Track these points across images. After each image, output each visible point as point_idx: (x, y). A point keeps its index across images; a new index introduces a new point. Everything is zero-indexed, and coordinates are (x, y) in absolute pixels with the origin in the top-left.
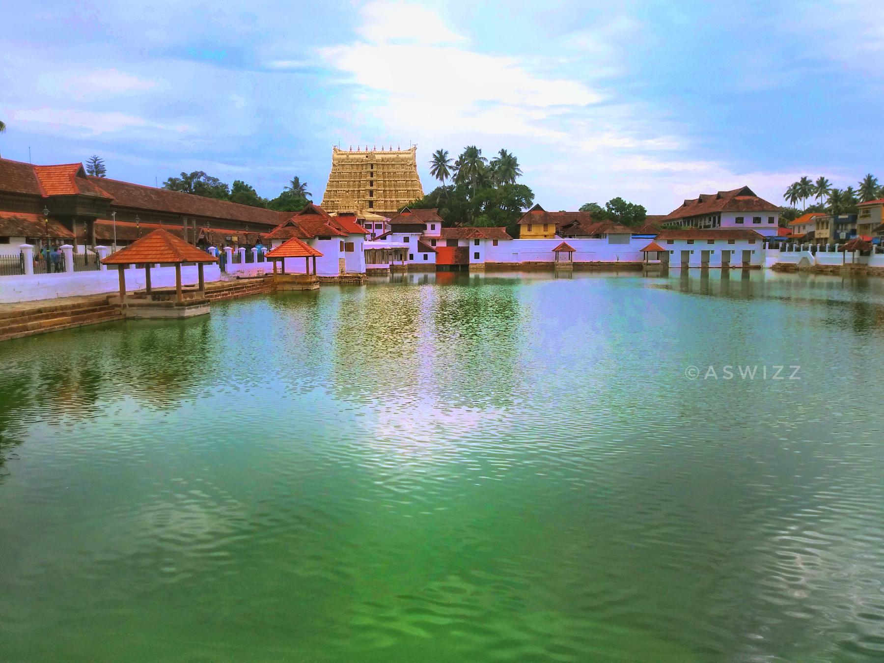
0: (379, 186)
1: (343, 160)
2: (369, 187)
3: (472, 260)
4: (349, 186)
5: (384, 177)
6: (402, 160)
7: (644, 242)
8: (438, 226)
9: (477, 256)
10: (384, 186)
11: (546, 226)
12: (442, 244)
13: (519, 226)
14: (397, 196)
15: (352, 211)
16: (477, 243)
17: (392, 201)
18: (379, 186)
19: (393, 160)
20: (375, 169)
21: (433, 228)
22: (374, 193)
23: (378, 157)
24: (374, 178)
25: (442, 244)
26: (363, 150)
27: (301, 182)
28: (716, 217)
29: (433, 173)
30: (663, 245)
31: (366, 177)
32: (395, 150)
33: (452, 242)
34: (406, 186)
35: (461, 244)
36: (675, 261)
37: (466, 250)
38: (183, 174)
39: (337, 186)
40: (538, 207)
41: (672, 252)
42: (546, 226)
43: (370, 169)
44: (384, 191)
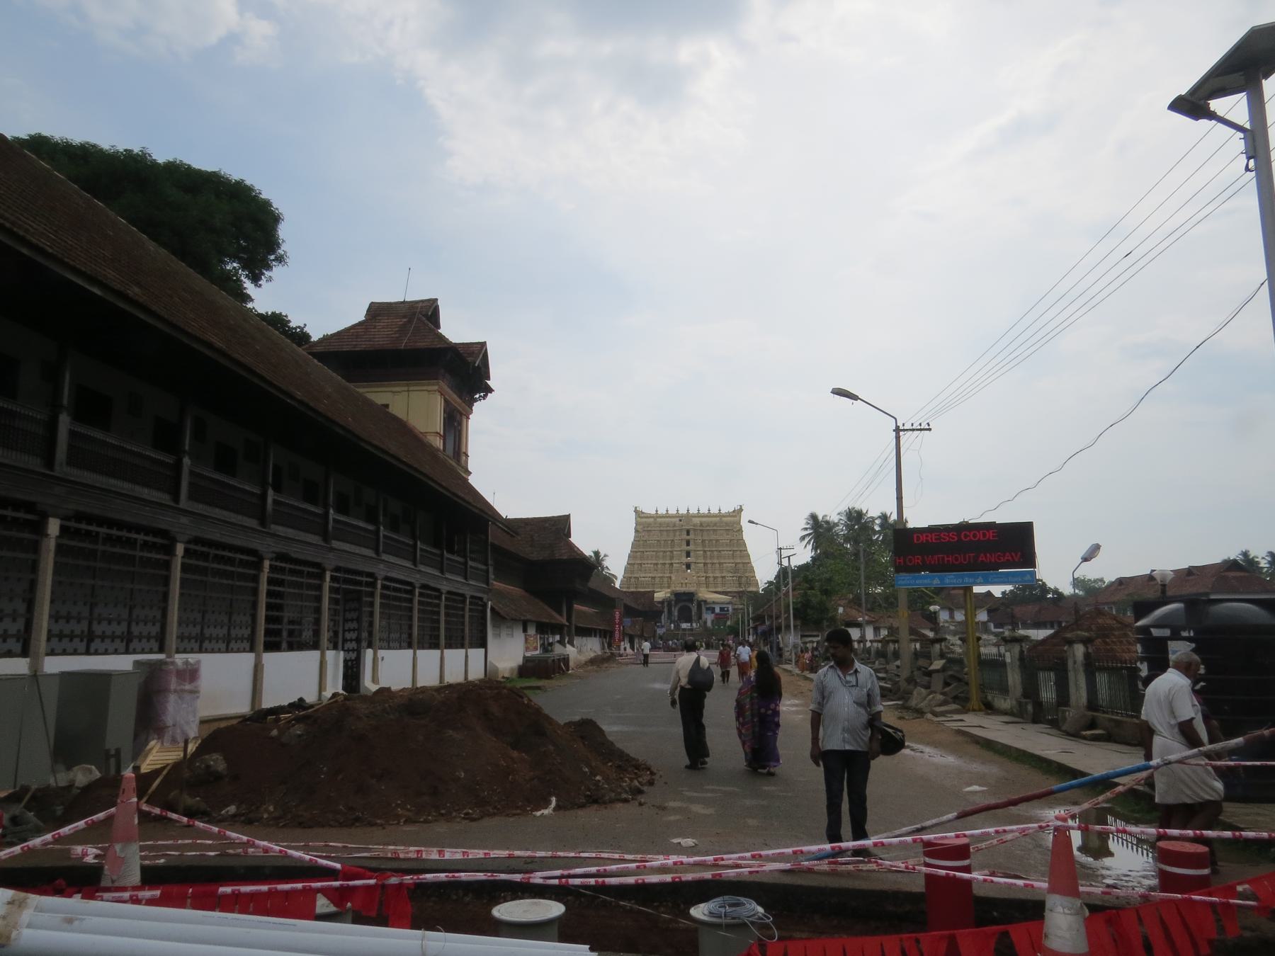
0: (697, 557)
1: (649, 525)
2: (685, 560)
4: (657, 557)
5: (704, 546)
6: (727, 524)
10: (705, 557)
14: (721, 571)
15: (691, 589)
17: (715, 578)
18: (697, 557)
19: (715, 524)
20: (692, 536)
22: (693, 566)
23: (696, 521)
24: (691, 547)
26: (672, 511)
27: (602, 555)
29: (803, 538)
31: (680, 545)
32: (714, 511)
34: (733, 557)
39: (642, 558)
43: (685, 536)
44: (705, 564)
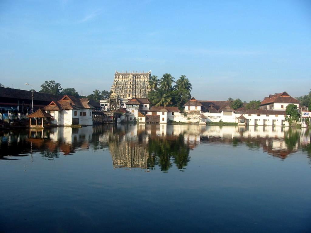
3: (161, 121)
7: (239, 115)
8: (148, 106)
9: (163, 119)
11: (196, 106)
12: (150, 113)
13: (185, 106)
16: (163, 114)
21: (146, 106)
25: (150, 113)
28: (271, 104)
30: (246, 116)
33: (154, 112)
35: (158, 113)
36: (252, 123)
37: (159, 117)
38: (47, 82)
40: (193, 98)
41: (250, 120)
42: (196, 106)
